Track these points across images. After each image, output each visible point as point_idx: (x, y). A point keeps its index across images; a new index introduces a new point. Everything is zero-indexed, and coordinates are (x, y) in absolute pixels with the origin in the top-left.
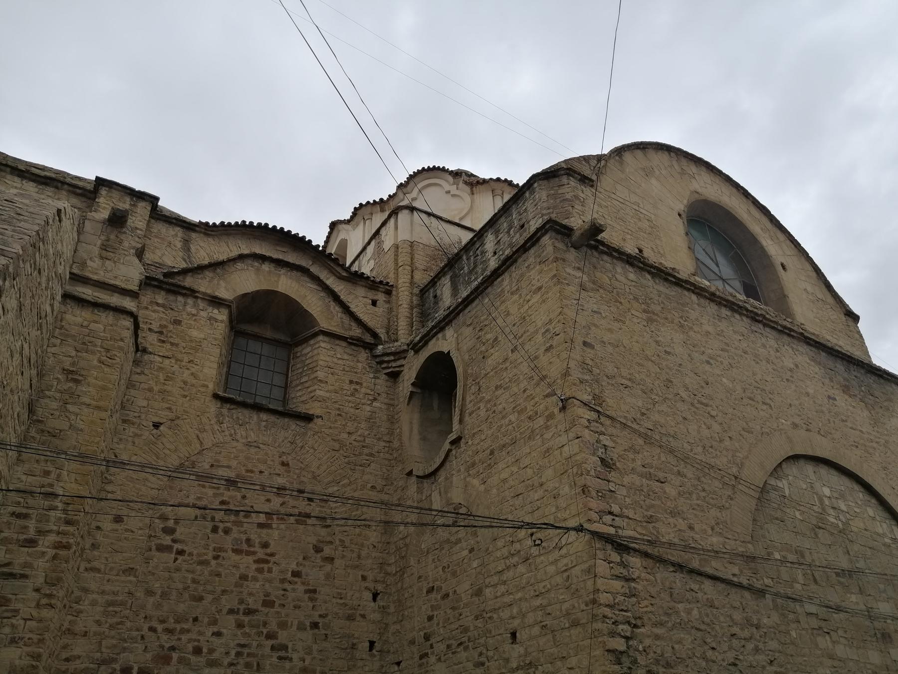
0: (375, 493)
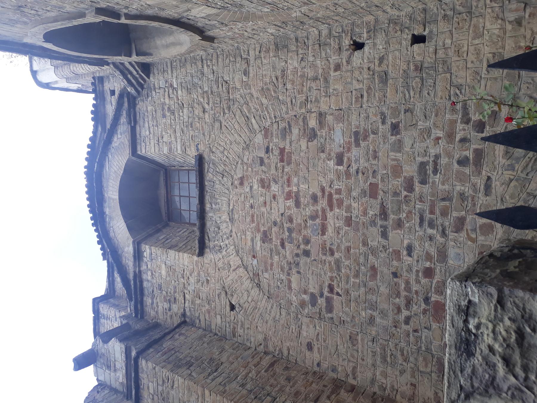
0: (251, 68)
